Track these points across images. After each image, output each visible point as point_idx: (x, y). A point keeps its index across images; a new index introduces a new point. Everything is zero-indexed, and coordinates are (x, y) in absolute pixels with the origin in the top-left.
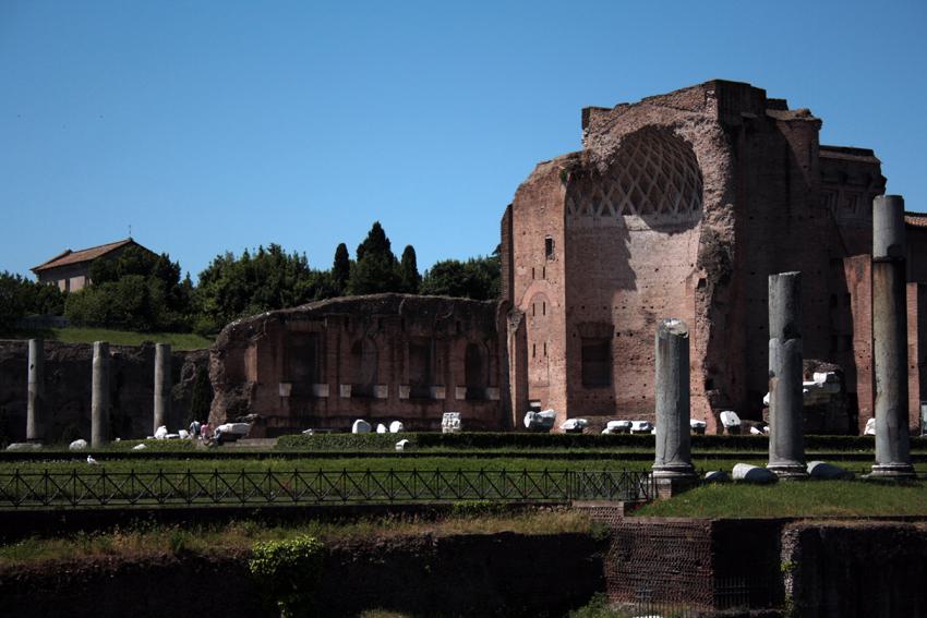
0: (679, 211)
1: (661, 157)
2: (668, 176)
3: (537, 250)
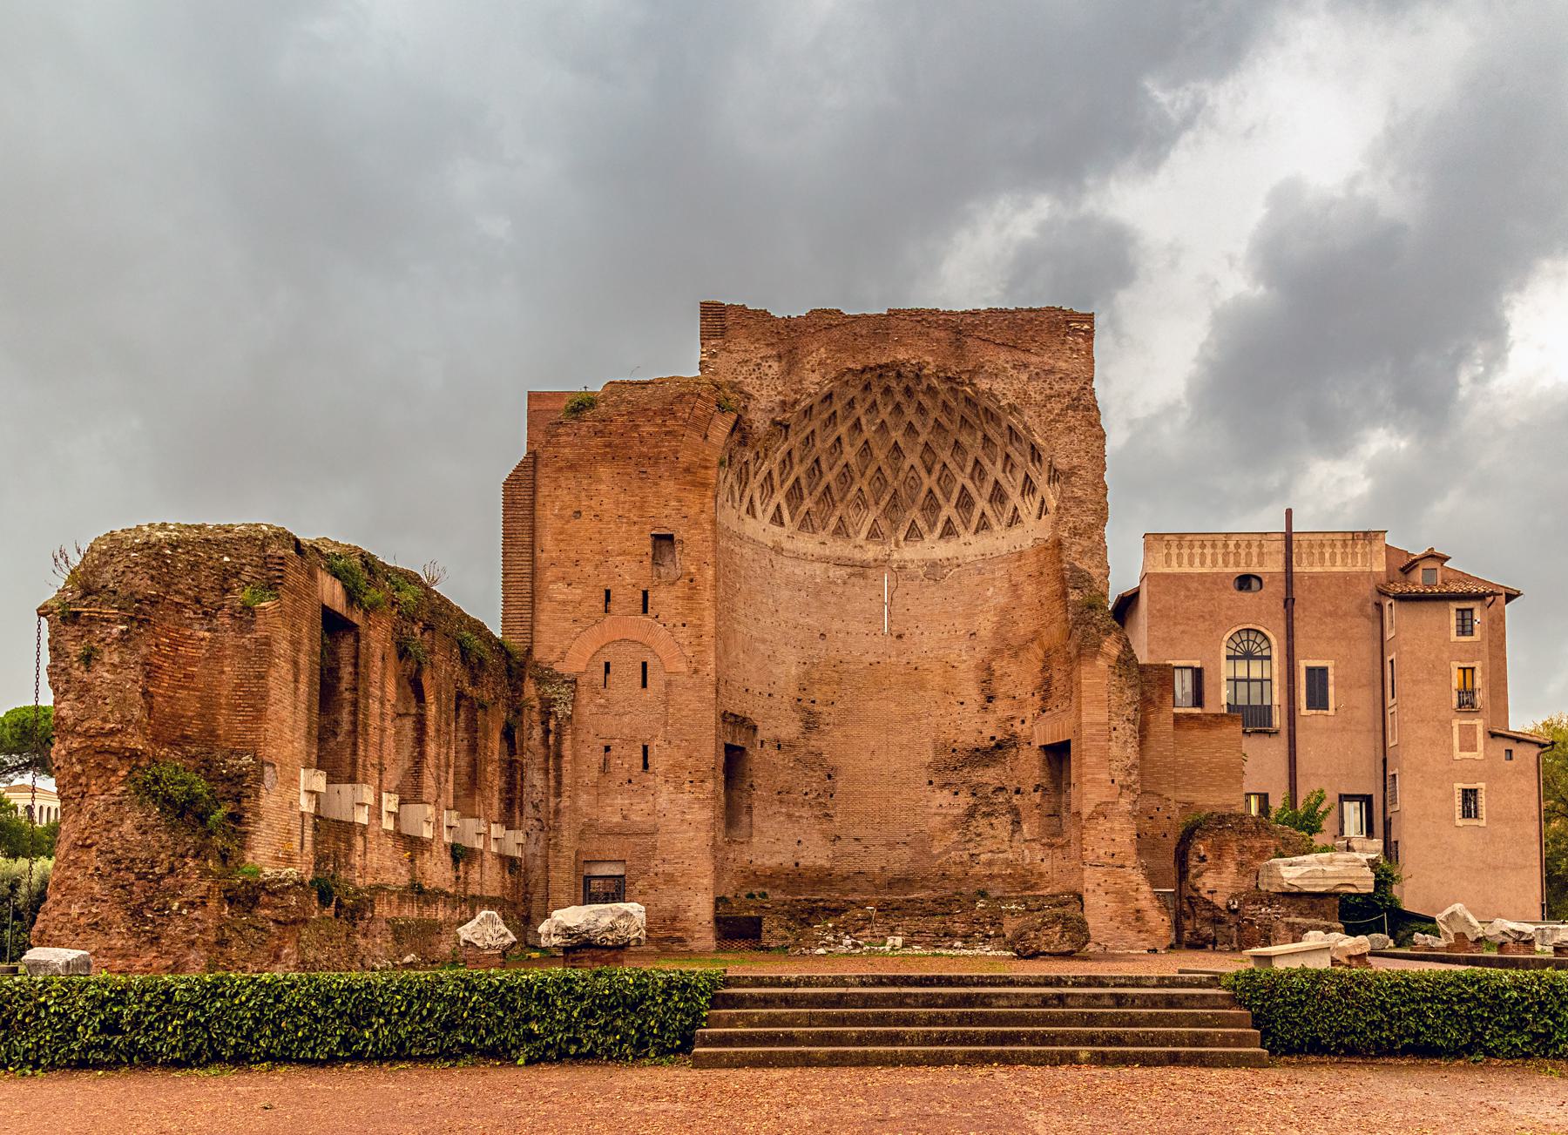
0: (867, 539)
2: (863, 475)
3: (624, 553)
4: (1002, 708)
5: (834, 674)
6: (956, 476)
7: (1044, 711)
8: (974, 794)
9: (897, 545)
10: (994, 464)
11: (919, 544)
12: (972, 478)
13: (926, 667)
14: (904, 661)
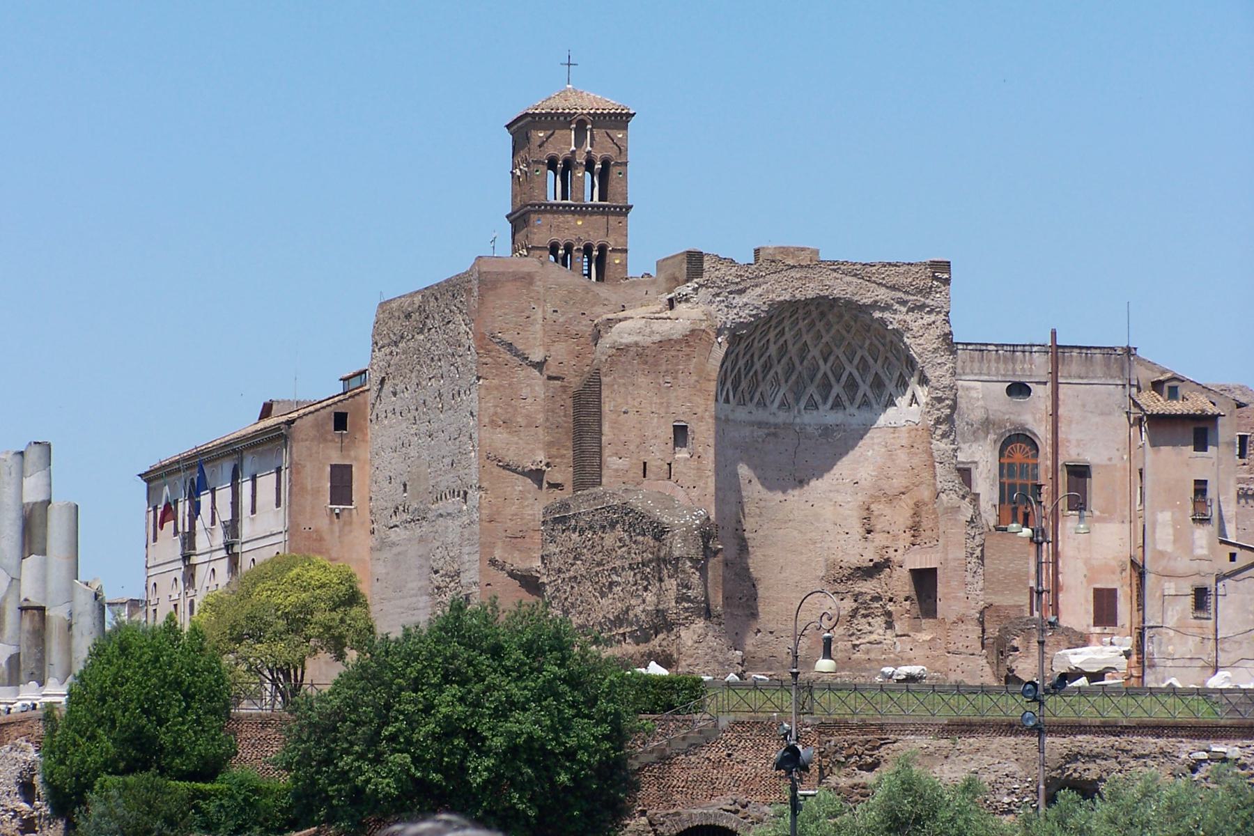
0: (779, 408)
1: (788, 335)
2: (779, 361)
4: (879, 539)
5: (758, 511)
6: (846, 366)
7: (914, 545)
8: (856, 601)
9: (799, 411)
10: (876, 362)
11: (815, 412)
12: (858, 369)
13: (821, 504)
14: (805, 499)
